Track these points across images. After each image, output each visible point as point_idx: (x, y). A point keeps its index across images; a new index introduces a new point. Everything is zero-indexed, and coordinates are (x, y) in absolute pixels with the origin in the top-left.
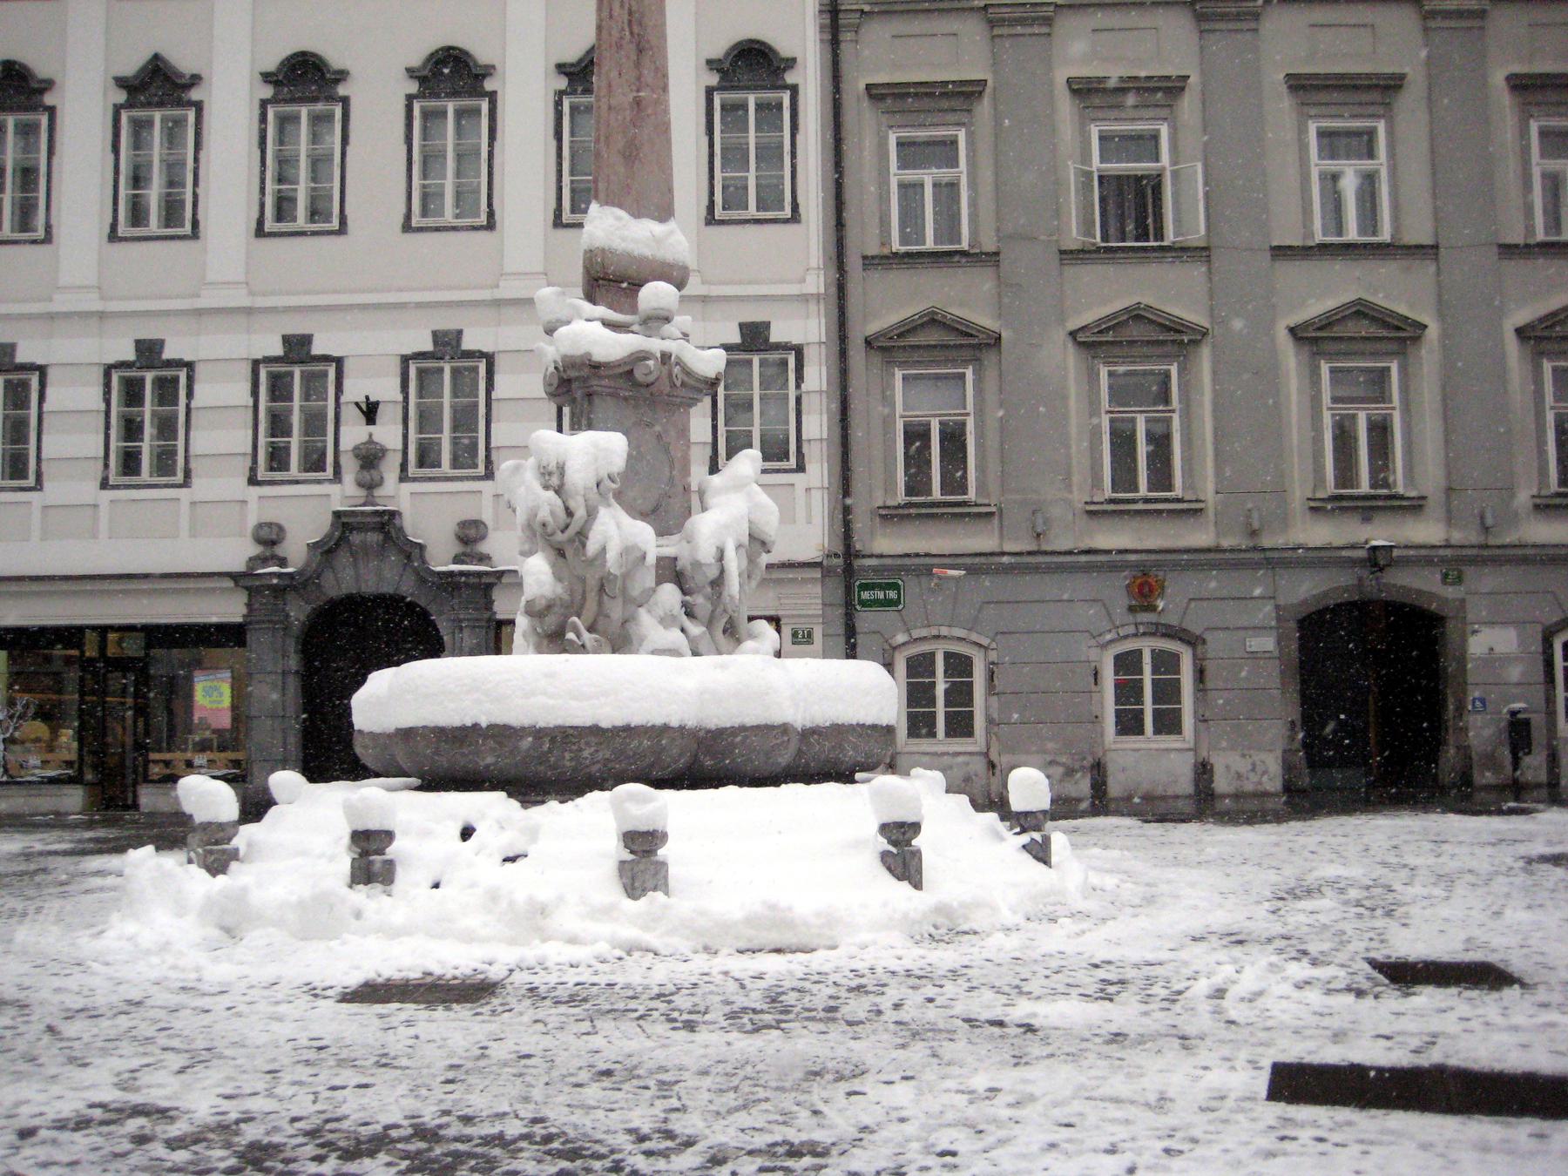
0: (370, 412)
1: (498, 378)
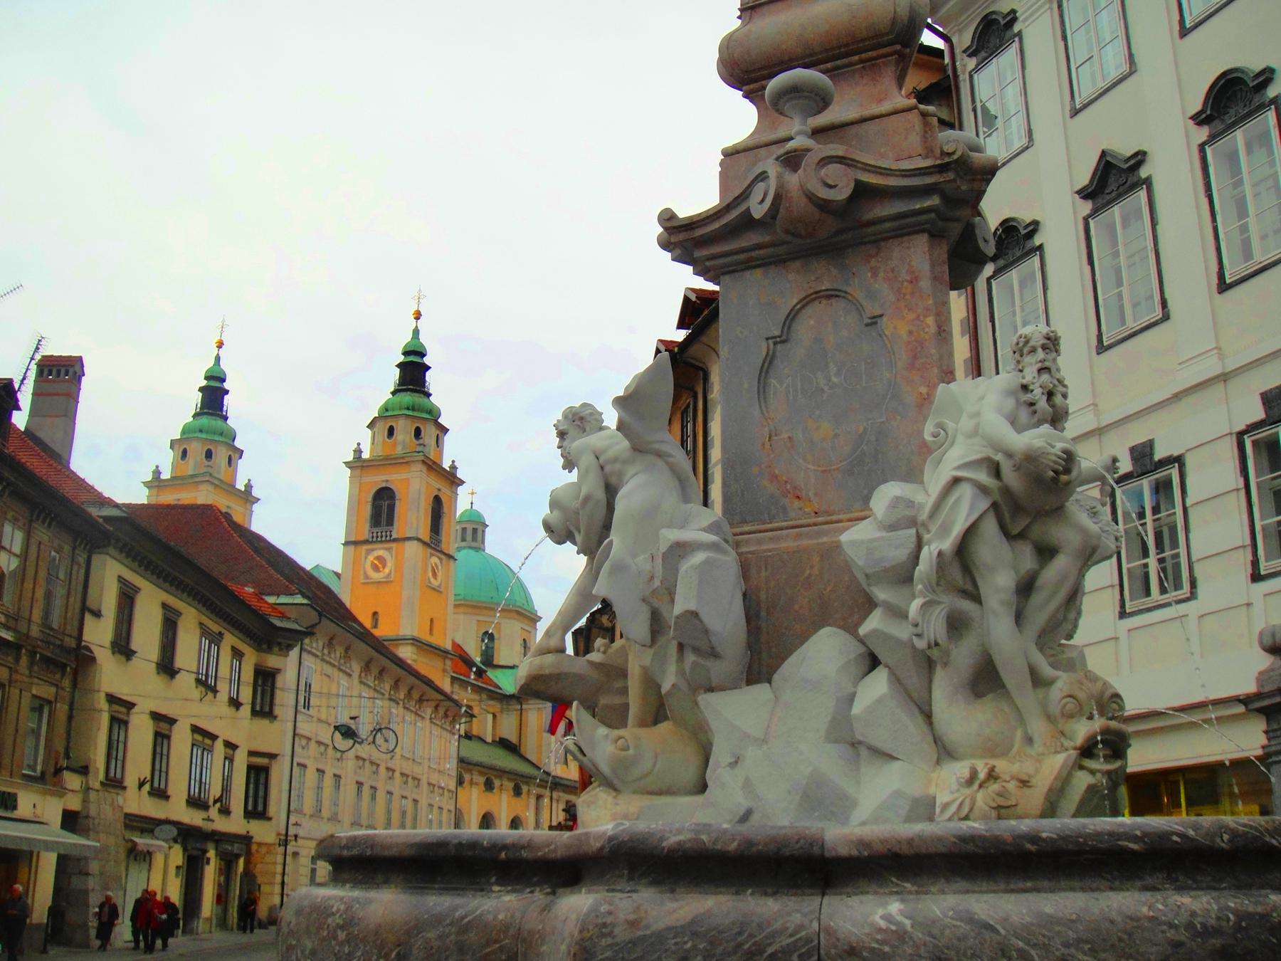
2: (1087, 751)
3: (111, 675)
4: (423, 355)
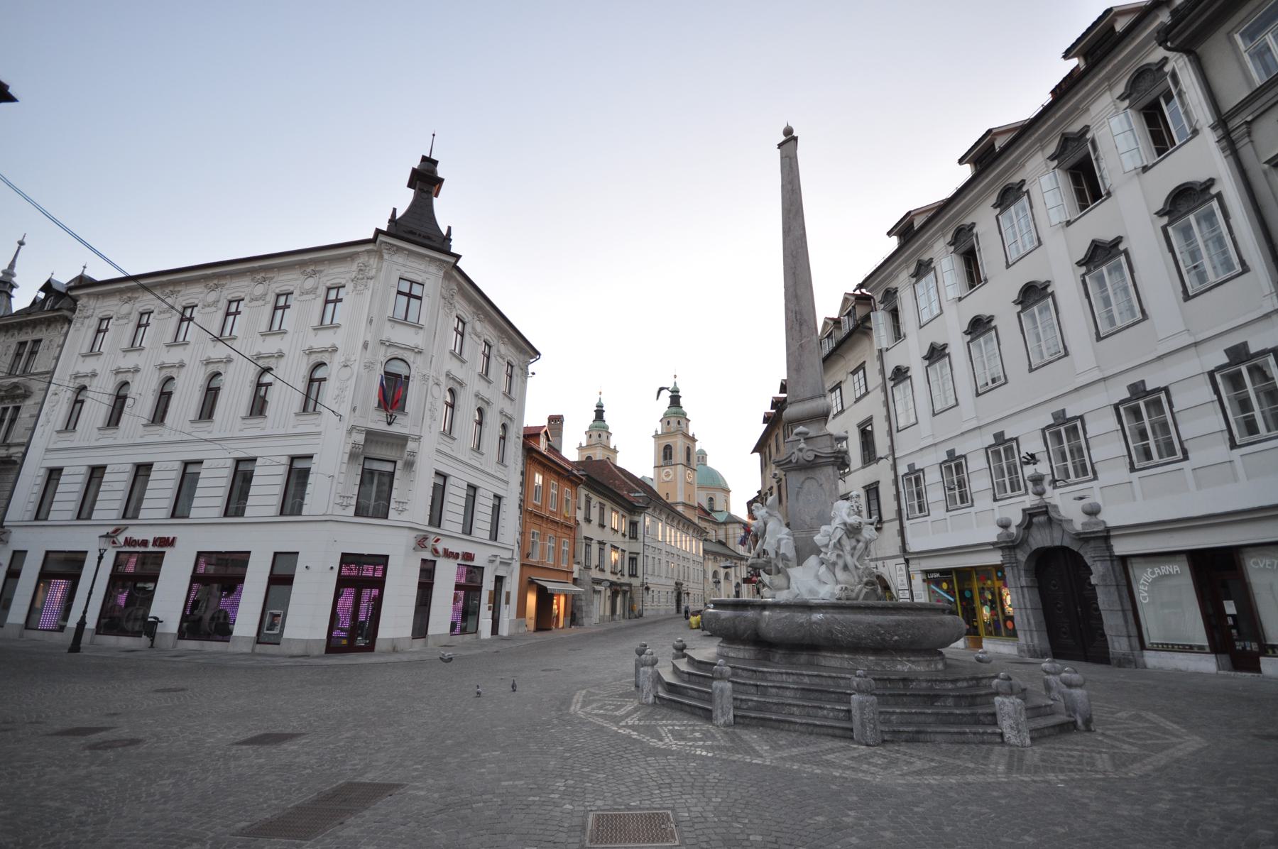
0: (1032, 459)
1: (1087, 427)
2: (866, 584)
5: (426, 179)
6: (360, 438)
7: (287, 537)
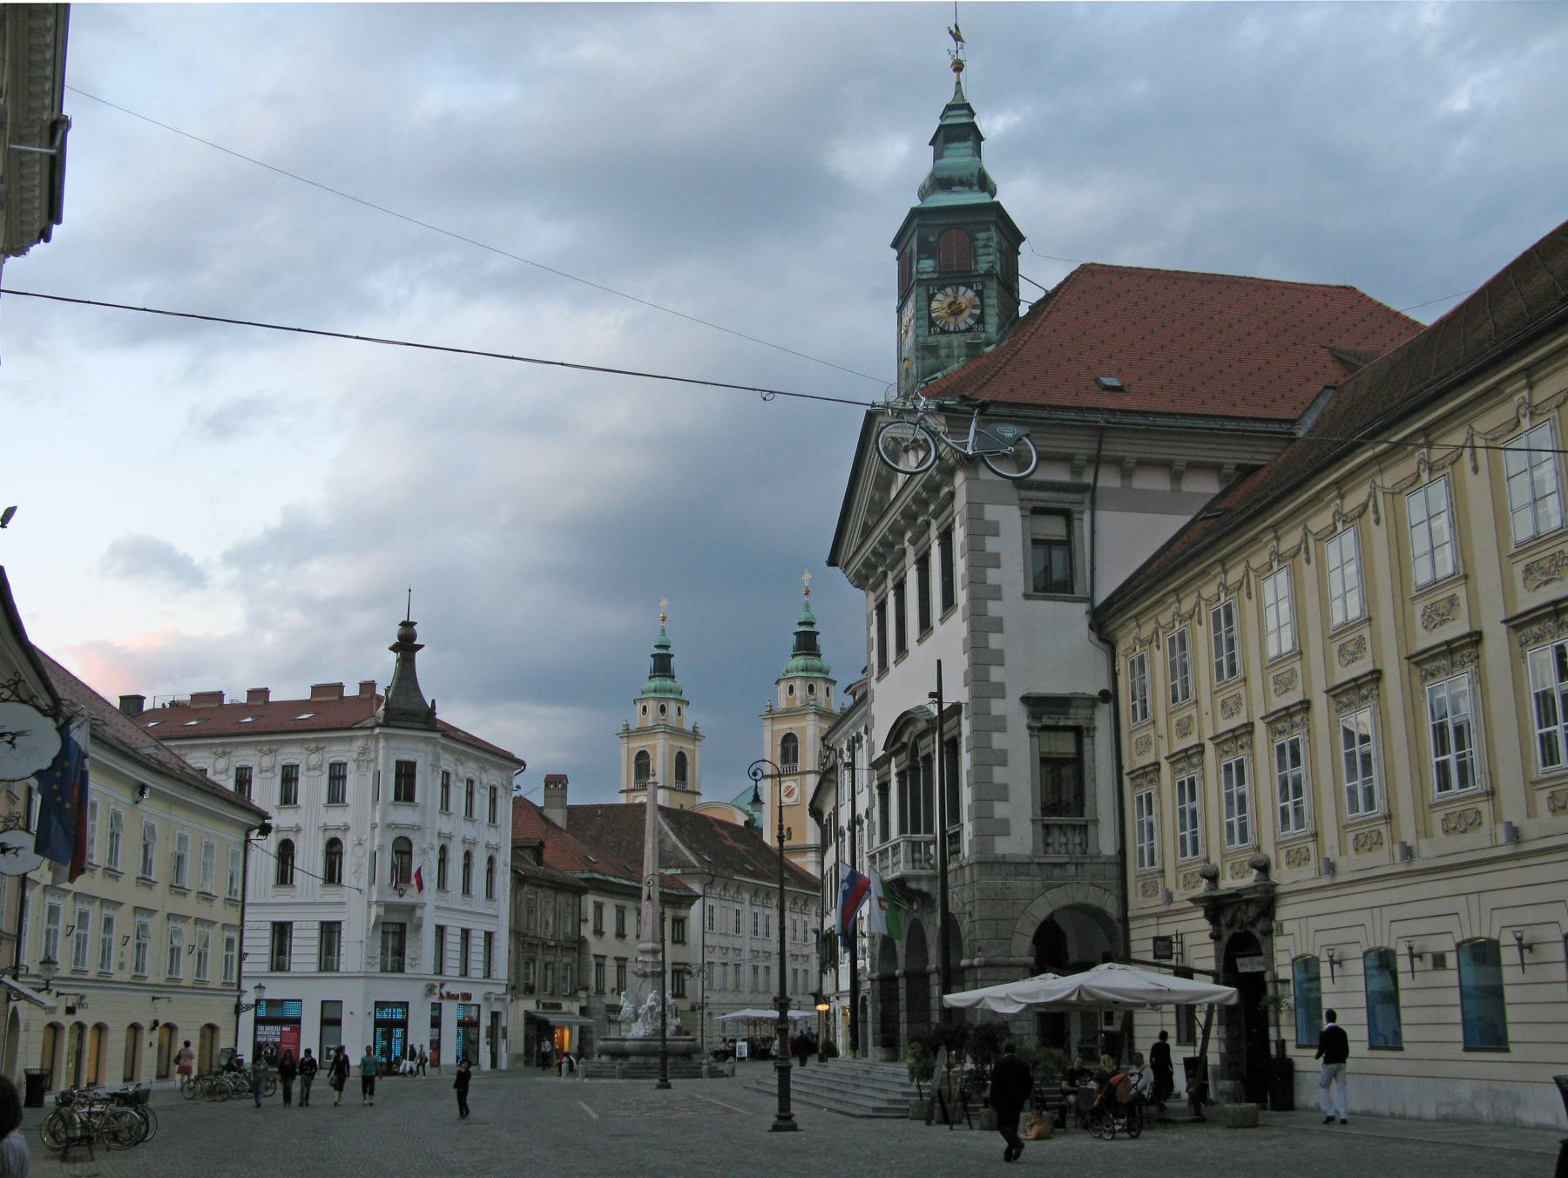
3: (595, 946)
4: (811, 624)
5: (406, 645)
6: (382, 911)
7: (330, 989)
